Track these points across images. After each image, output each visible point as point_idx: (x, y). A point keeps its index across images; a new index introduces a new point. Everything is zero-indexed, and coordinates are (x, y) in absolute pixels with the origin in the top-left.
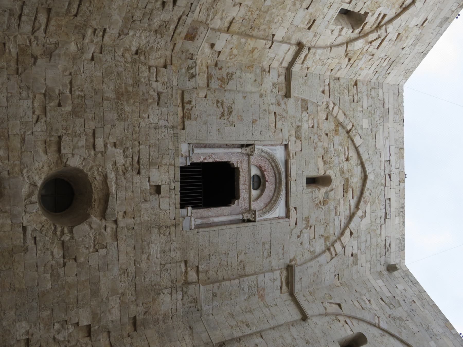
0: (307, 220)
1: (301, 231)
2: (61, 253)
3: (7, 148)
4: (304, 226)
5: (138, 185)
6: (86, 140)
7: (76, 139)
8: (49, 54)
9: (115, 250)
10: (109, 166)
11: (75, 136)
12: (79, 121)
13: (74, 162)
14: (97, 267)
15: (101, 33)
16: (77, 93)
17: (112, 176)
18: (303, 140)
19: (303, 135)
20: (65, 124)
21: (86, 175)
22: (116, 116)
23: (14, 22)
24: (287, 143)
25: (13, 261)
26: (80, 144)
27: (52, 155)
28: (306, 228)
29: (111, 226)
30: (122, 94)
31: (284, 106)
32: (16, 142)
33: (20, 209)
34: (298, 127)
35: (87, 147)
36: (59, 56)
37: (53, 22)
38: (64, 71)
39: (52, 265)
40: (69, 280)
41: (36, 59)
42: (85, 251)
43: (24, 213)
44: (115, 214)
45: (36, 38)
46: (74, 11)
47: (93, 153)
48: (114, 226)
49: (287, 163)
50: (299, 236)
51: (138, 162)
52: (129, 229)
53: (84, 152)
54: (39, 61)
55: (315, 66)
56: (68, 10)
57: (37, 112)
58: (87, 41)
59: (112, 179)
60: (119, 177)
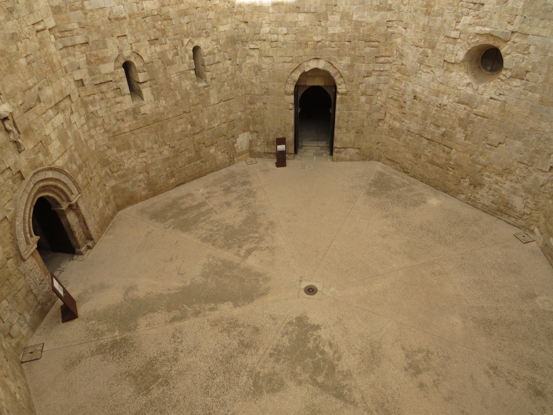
2: (518, 80)
3: (444, 93)
5: (491, 7)
6: (450, 43)
7: (448, 51)
8: (401, 56)
9: (536, 38)
10: (471, 30)
11: (446, 51)
12: (438, 46)
13: (461, 55)
14: (542, 57)
15: (391, 23)
16: (422, 44)
17: (478, 29)
20: (438, 56)
21: (473, 48)
22: (439, 18)
23: (384, 73)
25: (509, 111)
26: (451, 49)
27: (456, 68)
29: (514, 38)
30: (427, 10)
32: (442, 88)
33: (479, 97)
35: (455, 44)
36: (402, 50)
37: (383, 54)
38: (410, 48)
39: (524, 89)
40: (540, 80)
41: (402, 64)
42: (524, 63)
43: (482, 96)
44: (506, 32)
45: (394, 61)
46: (376, 44)
47: (459, 41)
48: (516, 34)
51: (475, 4)
52: (523, 22)
53: (458, 47)
54: (404, 63)
56: (376, 47)
57: (429, 71)
58: (396, 31)
59: (481, 30)
60: (480, 24)
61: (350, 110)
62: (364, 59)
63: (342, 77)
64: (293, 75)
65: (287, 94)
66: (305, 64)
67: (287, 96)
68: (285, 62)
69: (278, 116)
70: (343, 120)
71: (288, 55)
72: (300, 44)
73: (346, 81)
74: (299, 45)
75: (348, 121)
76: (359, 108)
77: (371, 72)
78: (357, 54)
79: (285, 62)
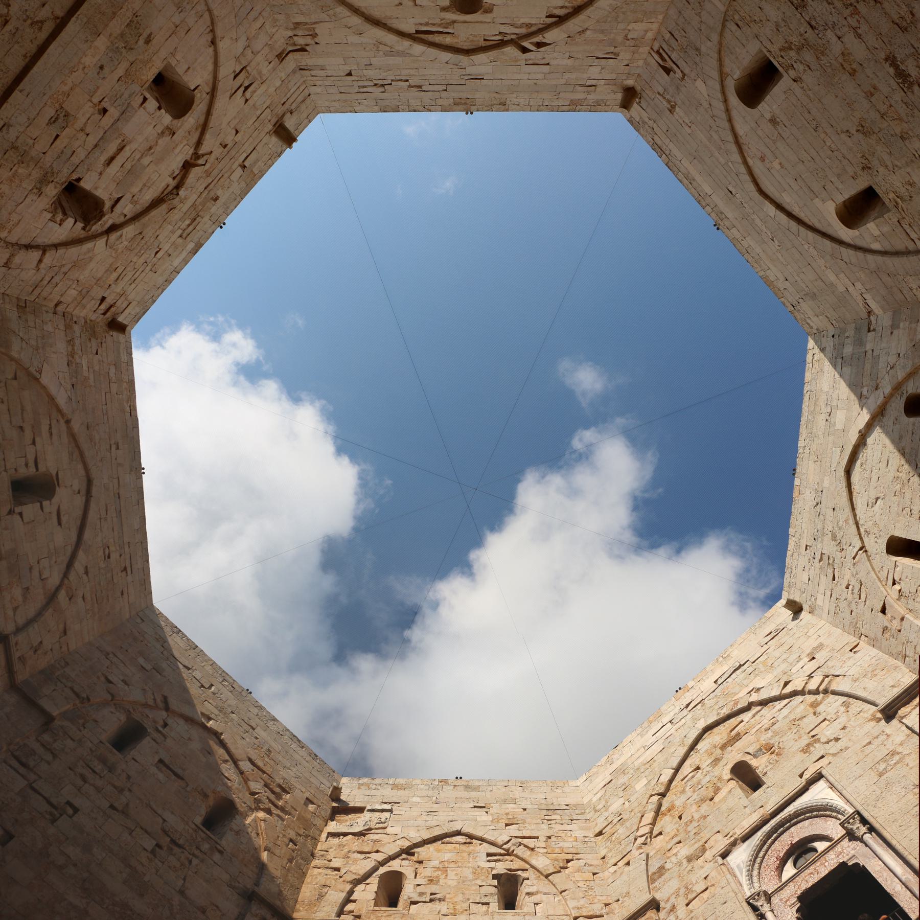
0: (806, 750)
1: (827, 743)
4: (817, 745)
18: (704, 840)
19: (697, 846)
24: (719, 858)
28: (818, 741)
31: (673, 900)
34: (689, 859)
49: (745, 838)
50: (837, 740)
55: (598, 897)
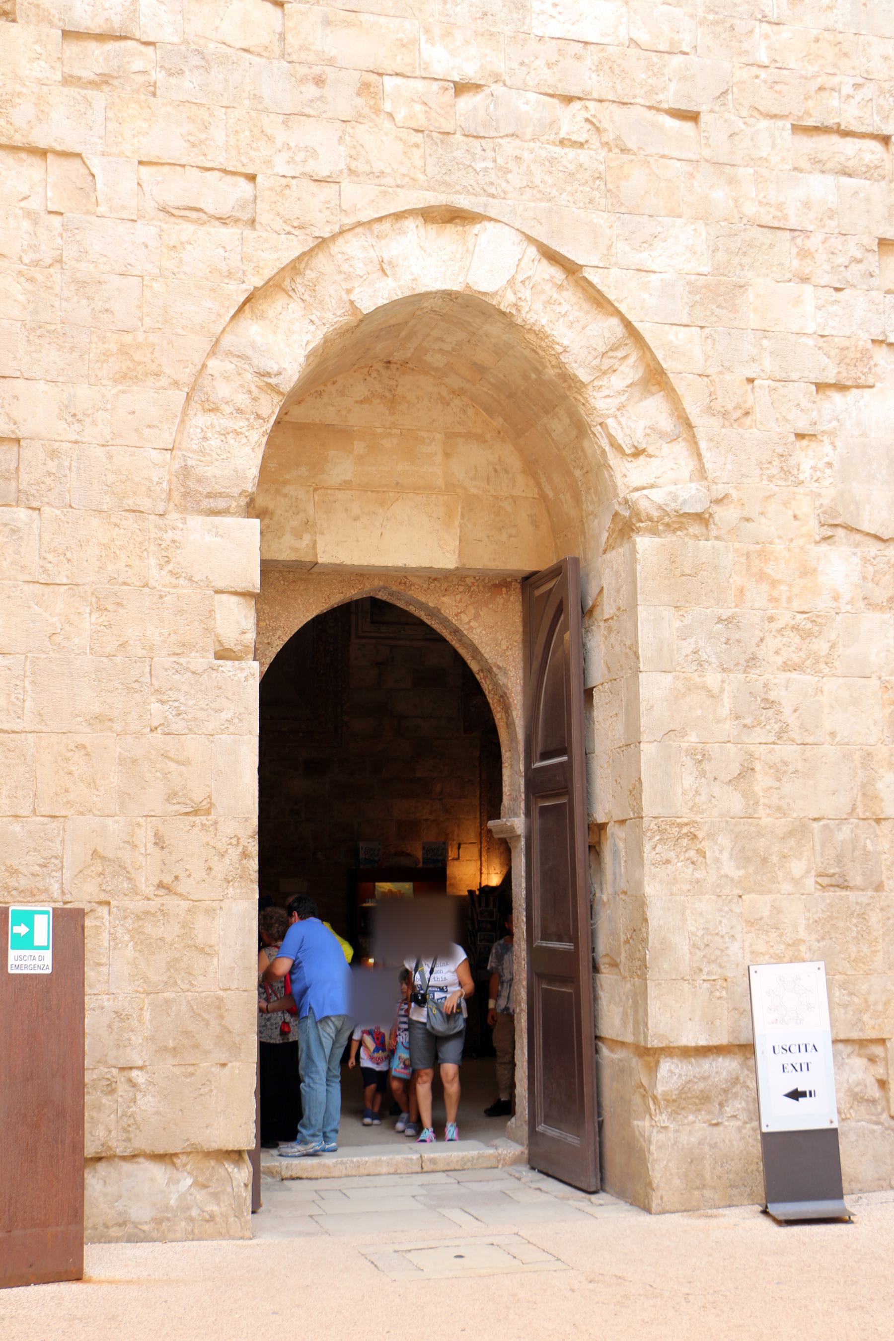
46: (872, 150)
61: (752, 661)
62: (805, 254)
63: (655, 378)
64: (252, 330)
65: (193, 496)
66: (354, 247)
67: (196, 522)
68: (192, 212)
69: (100, 720)
70: (700, 757)
71: (220, 159)
72: (319, 81)
73: (693, 410)
74: (311, 90)
75: (747, 771)
76: (821, 646)
77: (865, 355)
78: (750, 209)
79: (192, 212)
